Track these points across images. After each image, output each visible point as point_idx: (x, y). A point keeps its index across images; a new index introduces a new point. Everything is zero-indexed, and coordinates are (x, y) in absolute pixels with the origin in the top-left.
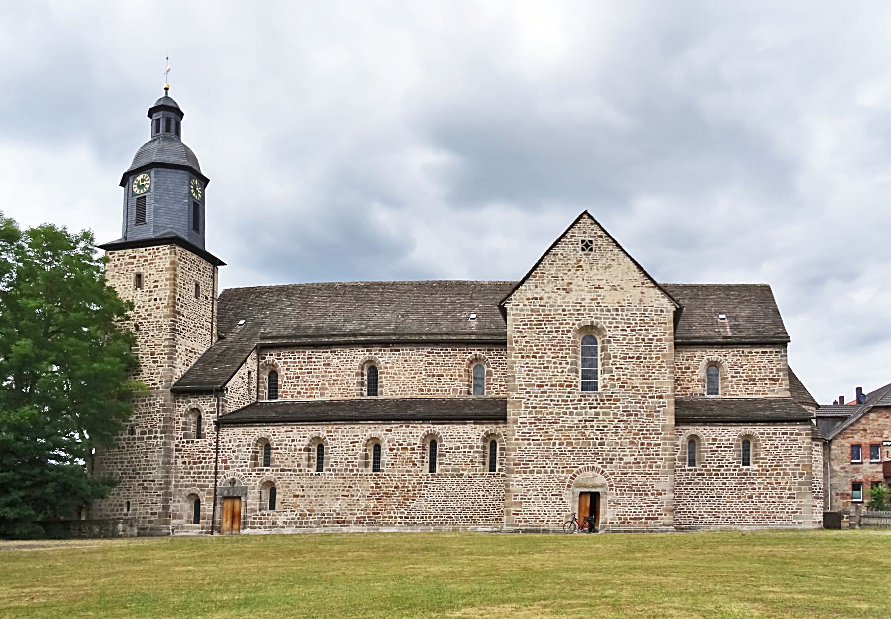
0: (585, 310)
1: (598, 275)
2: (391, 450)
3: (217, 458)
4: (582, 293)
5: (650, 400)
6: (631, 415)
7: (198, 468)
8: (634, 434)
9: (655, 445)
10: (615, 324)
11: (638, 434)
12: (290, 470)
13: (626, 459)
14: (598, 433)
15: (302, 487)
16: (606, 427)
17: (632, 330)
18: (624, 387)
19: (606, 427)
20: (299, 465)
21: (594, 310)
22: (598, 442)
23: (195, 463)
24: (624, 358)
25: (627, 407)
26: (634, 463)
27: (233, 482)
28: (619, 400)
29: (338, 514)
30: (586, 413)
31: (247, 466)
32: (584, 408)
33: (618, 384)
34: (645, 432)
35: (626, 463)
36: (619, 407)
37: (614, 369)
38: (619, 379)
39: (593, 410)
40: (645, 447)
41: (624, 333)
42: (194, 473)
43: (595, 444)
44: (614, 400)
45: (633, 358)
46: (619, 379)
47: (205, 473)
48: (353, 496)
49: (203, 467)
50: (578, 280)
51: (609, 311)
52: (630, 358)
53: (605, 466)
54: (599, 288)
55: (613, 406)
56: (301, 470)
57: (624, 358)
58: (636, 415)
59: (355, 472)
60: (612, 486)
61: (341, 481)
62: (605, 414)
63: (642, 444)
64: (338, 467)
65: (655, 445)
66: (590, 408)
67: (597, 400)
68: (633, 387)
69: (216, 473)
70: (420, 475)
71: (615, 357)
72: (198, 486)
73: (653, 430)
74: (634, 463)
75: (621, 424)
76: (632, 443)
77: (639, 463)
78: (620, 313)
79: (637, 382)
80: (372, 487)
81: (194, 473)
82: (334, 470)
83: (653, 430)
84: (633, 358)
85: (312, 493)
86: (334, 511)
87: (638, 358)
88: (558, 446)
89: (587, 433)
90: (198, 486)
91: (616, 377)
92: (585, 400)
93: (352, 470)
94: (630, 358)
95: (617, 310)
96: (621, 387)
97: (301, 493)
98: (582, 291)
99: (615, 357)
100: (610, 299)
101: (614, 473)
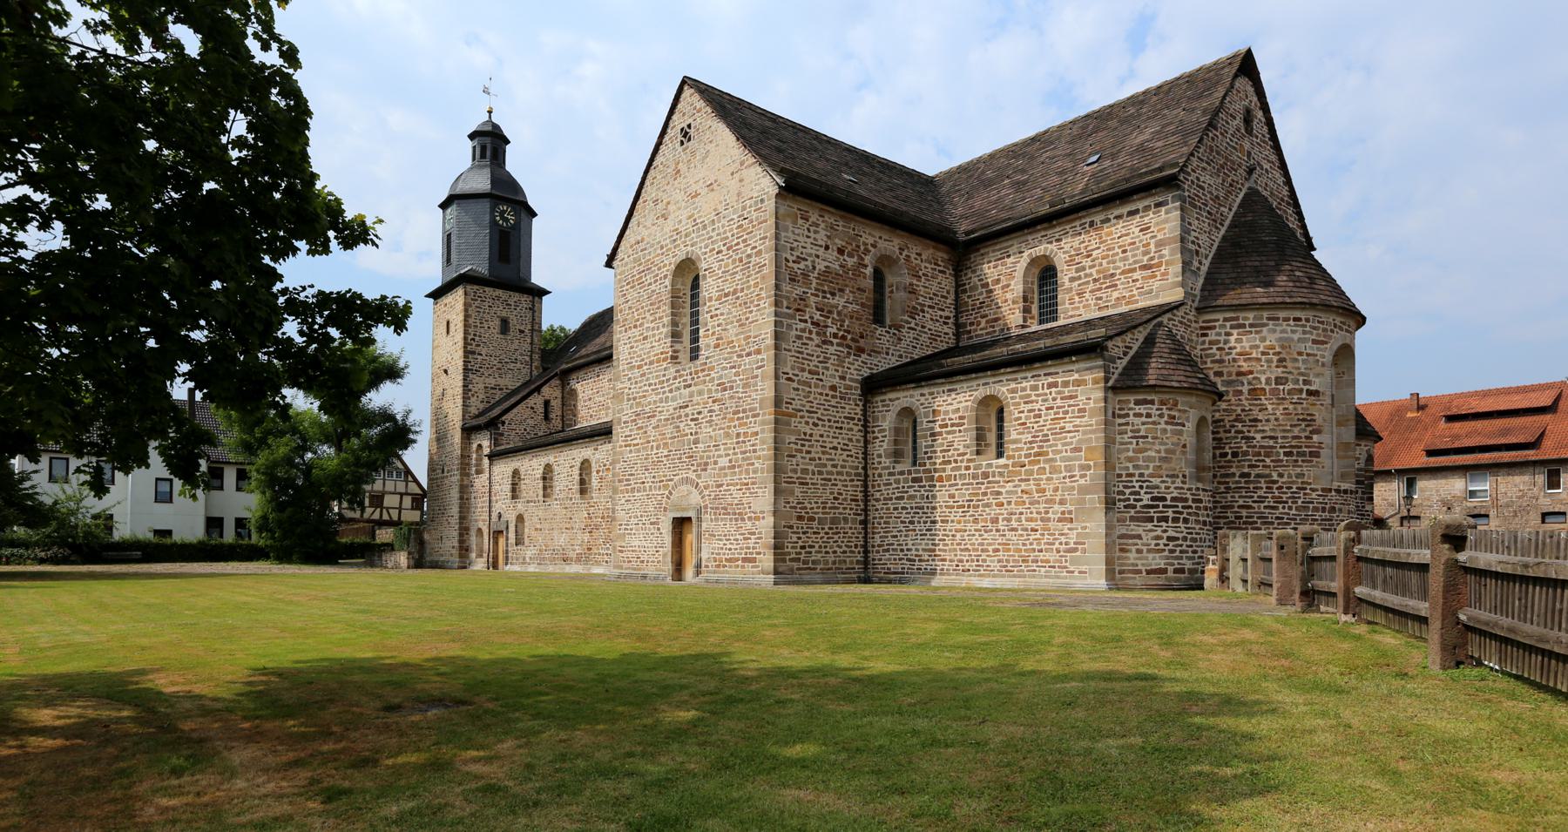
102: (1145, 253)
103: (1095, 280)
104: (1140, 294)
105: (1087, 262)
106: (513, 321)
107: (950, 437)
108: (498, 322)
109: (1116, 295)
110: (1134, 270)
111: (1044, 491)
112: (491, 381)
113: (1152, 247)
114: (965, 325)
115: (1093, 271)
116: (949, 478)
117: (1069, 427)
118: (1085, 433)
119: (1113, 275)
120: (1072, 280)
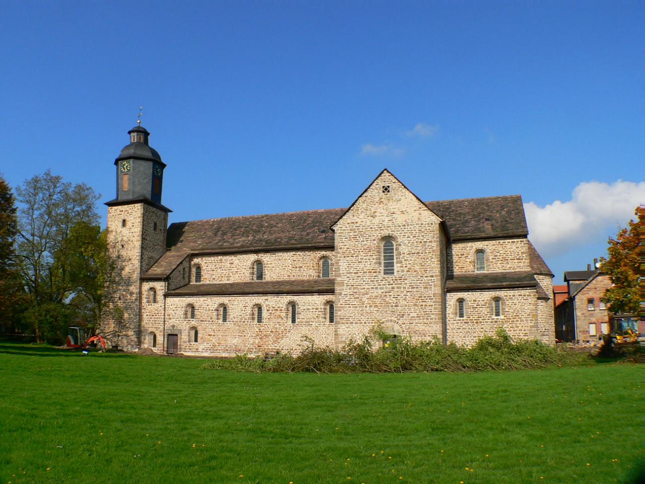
0: (384, 227)
1: (392, 206)
2: (268, 310)
3: (164, 313)
4: (383, 217)
5: (426, 279)
6: (414, 288)
7: (155, 318)
8: (417, 300)
9: (430, 306)
10: (403, 234)
11: (418, 300)
12: (206, 321)
13: (412, 315)
14: (394, 299)
15: (213, 330)
16: (399, 295)
17: (413, 237)
18: (409, 271)
19: (399, 295)
20: (211, 318)
21: (390, 227)
22: (394, 305)
23: (153, 316)
24: (409, 254)
25: (411, 283)
26: (417, 317)
27: (173, 326)
28: (406, 279)
29: (236, 346)
30: (386, 288)
31: (181, 318)
32: (385, 285)
33: (406, 269)
34: (423, 298)
35: (412, 317)
36: (406, 284)
37: (403, 261)
38: (406, 267)
39: (391, 286)
40: (423, 307)
41: (409, 239)
42: (153, 321)
43: (392, 306)
44: (404, 279)
45: (414, 253)
46: (406, 267)
47: (158, 321)
48: (245, 336)
49: (157, 318)
50: (380, 210)
51: (399, 226)
52: (413, 253)
53: (399, 319)
54: (394, 213)
55: (403, 283)
56: (213, 321)
57: (409, 254)
58: (417, 288)
59: (246, 323)
60: (404, 331)
61: (238, 328)
62: (398, 288)
63: (422, 305)
64: (236, 320)
65: (430, 306)
66: (389, 285)
67: (393, 280)
68: (415, 271)
69: (164, 321)
70: (286, 324)
71: (404, 254)
72: (155, 328)
73: (428, 297)
74: (417, 317)
75: (409, 294)
76: (415, 305)
77: (420, 317)
78: (406, 227)
79: (417, 268)
80: (257, 332)
81: (153, 321)
82: (233, 322)
83: (428, 297)
84: (414, 253)
85: (220, 334)
86: (234, 344)
87: (418, 253)
88: (368, 308)
89: (387, 300)
90: (155, 328)
91: (404, 266)
92: (386, 280)
93: (244, 322)
94: (413, 253)
95: (405, 226)
96: (407, 271)
97: (213, 334)
98: (383, 216)
99: (404, 254)
100: (400, 219)
101: (405, 323)
102: (518, 255)
103: (501, 260)
104: (517, 267)
105: (498, 254)
106: (158, 224)
107: (481, 309)
108: (153, 224)
109: (509, 266)
110: (514, 259)
111: (518, 327)
112: (150, 254)
113: (520, 253)
114: (449, 268)
115: (501, 257)
116: (481, 322)
117: (526, 308)
118: (531, 310)
119: (508, 260)
120: (493, 259)
